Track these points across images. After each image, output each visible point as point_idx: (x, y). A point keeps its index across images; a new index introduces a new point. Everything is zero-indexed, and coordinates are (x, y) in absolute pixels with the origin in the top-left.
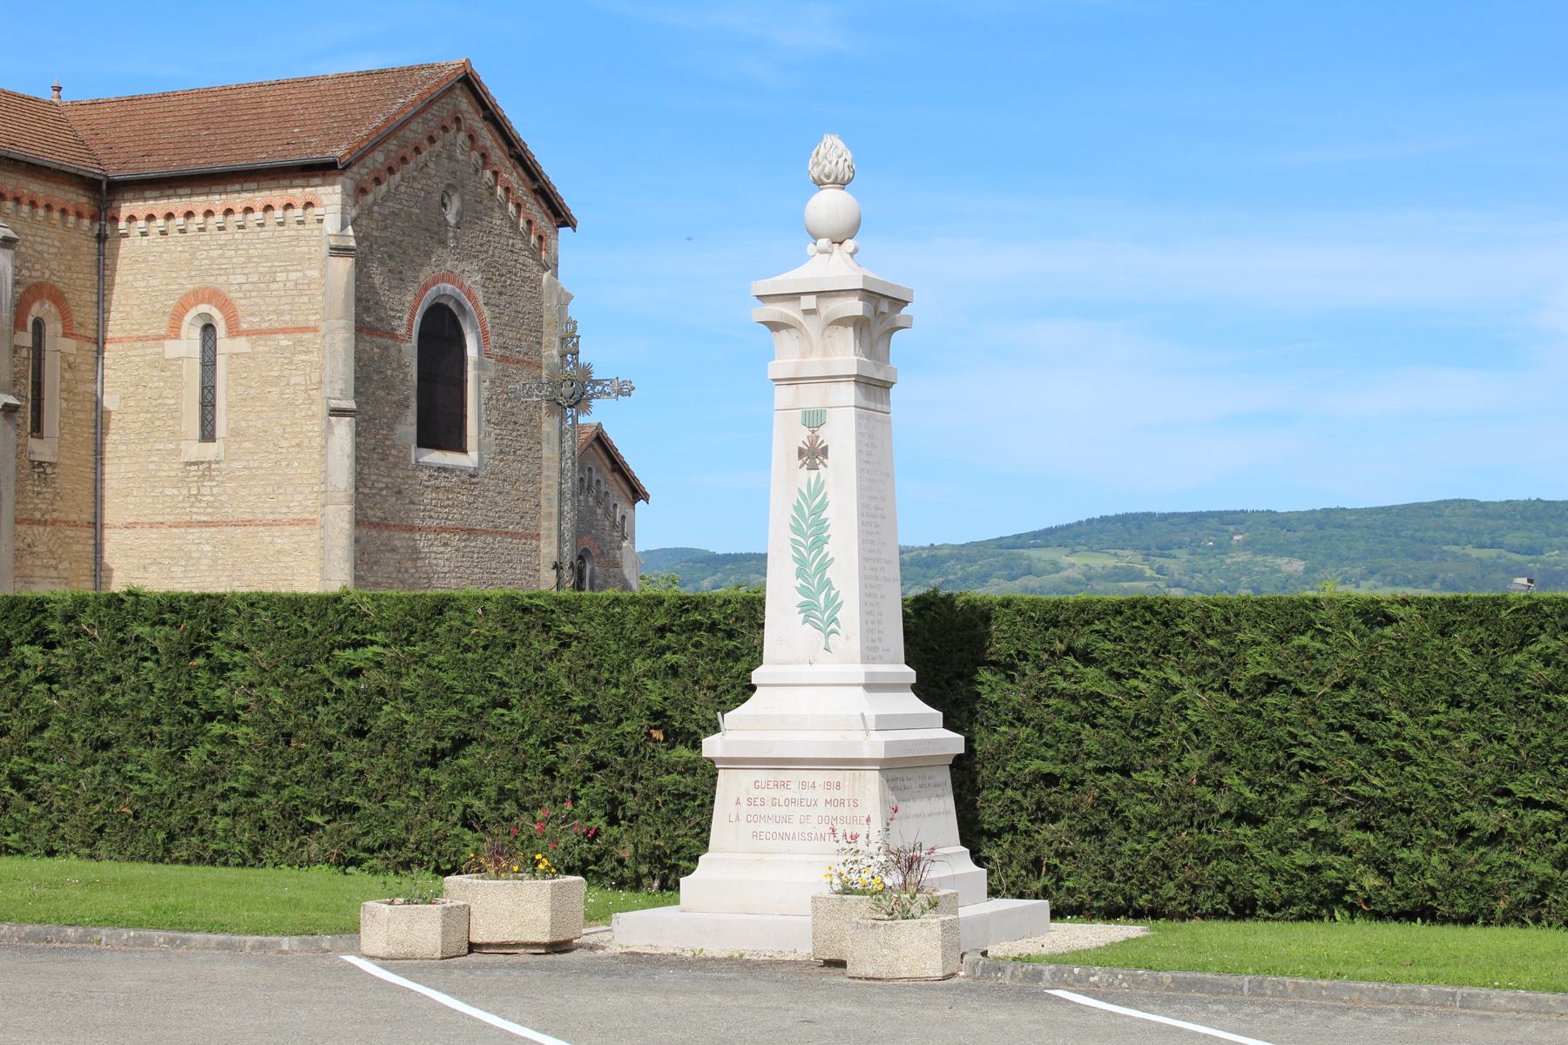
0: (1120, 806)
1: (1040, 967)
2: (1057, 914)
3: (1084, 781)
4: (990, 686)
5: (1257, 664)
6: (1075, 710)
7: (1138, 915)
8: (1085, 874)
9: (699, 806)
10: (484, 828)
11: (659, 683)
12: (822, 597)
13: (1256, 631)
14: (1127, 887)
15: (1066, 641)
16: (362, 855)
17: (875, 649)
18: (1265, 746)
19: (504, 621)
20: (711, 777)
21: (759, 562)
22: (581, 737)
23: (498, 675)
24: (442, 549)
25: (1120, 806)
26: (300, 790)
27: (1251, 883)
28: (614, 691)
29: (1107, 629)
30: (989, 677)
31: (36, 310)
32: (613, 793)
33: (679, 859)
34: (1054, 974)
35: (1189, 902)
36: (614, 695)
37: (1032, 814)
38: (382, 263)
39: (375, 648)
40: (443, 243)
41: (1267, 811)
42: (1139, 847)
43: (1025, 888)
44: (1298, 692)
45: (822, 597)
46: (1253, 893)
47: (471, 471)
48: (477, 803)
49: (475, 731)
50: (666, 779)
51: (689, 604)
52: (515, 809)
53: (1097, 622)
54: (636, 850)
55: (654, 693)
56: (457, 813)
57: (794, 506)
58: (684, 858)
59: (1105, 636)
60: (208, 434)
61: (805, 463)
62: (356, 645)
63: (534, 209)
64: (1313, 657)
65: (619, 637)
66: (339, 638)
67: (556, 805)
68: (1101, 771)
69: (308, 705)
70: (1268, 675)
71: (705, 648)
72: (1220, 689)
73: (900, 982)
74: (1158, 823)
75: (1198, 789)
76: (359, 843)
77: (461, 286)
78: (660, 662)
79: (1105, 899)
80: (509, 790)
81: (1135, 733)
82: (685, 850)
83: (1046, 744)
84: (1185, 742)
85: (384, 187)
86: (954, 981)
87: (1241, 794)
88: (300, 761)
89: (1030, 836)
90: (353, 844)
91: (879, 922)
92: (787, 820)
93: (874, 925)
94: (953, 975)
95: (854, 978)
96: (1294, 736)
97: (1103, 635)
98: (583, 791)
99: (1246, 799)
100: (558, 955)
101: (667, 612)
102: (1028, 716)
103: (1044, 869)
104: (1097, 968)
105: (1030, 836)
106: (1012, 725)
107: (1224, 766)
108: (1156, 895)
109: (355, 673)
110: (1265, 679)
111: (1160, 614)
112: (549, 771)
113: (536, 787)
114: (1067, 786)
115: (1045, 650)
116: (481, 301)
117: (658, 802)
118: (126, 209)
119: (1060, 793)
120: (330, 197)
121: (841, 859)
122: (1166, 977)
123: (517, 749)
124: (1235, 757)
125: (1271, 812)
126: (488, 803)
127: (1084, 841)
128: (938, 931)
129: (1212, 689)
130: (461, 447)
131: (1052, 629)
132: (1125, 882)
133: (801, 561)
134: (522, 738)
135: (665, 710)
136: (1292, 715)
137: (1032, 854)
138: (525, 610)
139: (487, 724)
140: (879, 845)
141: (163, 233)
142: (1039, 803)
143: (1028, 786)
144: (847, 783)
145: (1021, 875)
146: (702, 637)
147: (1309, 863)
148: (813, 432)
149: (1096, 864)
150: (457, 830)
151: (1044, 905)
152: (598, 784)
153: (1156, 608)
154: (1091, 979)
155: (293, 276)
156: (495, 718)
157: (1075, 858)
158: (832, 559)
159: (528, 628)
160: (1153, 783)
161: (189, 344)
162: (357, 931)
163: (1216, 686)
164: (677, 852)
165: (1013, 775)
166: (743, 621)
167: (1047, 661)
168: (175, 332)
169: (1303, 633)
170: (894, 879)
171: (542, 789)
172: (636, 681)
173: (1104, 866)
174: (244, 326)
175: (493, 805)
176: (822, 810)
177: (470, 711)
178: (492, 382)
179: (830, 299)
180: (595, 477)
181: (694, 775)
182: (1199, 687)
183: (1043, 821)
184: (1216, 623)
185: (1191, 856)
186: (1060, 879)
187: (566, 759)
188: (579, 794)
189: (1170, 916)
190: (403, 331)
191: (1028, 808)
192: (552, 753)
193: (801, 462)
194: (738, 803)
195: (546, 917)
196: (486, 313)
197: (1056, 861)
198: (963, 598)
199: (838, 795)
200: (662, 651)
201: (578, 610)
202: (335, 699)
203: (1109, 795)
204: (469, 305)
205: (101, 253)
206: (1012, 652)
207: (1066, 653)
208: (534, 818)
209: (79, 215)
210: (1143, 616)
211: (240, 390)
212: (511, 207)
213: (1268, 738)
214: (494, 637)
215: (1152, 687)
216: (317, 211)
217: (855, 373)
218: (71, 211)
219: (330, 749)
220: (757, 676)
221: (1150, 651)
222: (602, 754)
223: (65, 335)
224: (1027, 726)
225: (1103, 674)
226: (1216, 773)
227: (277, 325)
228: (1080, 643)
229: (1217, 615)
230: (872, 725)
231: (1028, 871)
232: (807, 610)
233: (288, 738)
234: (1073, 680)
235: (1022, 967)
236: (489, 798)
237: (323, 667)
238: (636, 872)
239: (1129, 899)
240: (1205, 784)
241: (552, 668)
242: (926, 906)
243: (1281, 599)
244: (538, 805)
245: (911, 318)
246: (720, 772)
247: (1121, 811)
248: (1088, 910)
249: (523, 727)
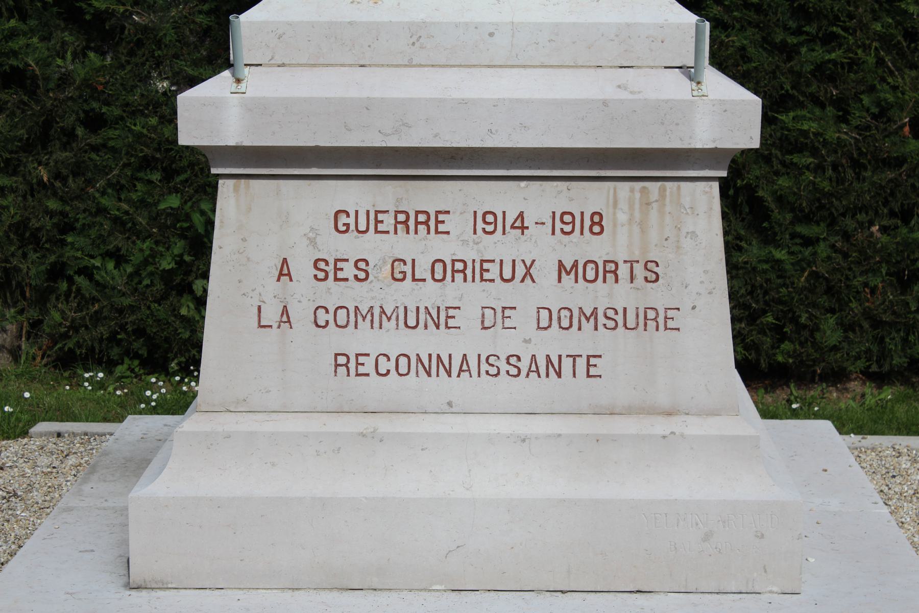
144: (622, 217)
194: (284, 272)
246: (225, 188)
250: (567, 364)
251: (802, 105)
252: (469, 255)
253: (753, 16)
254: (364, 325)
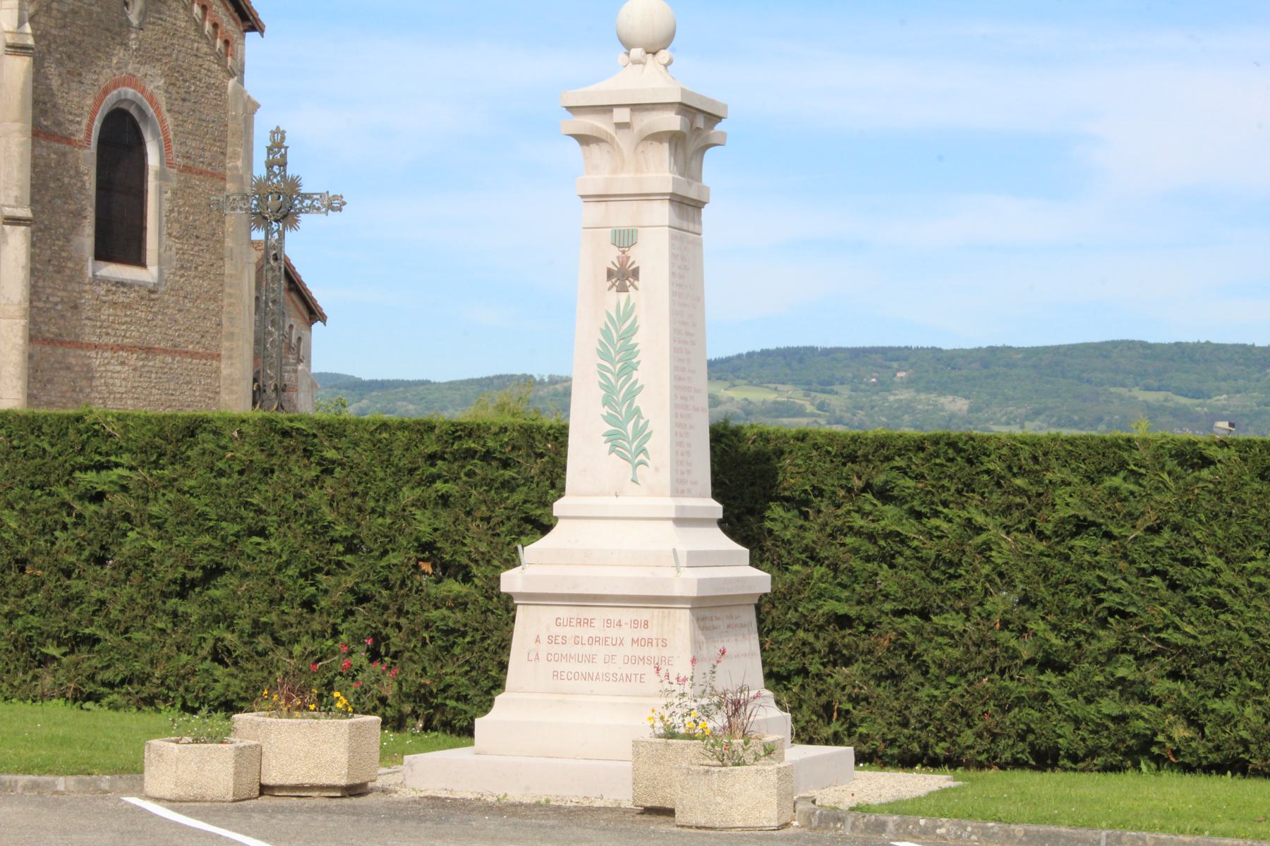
0: (919, 650)
1: (883, 818)
2: (862, 758)
3: (880, 623)
4: (782, 522)
5: (1067, 505)
6: (873, 550)
7: (934, 763)
8: (879, 720)
9: (468, 643)
10: (236, 663)
11: (428, 513)
12: (630, 426)
13: (1066, 471)
14: (923, 735)
15: (864, 478)
16: (102, 689)
17: (682, 482)
18: (1072, 591)
19: (262, 445)
20: (482, 613)
21: (561, 391)
22: (344, 568)
23: (255, 501)
24: (119, 368)
25: (919, 650)
26: (35, 620)
27: (1054, 732)
28: (380, 520)
29: (909, 466)
30: (782, 513)
32: (376, 628)
33: (446, 698)
34: (898, 826)
35: (987, 751)
36: (381, 525)
37: (825, 656)
38: (59, 63)
39: (120, 471)
41: (1073, 658)
42: (936, 693)
43: (815, 733)
44: (1109, 536)
45: (630, 426)
46: (1057, 743)
47: (151, 286)
48: (228, 636)
49: (227, 562)
50: (435, 614)
51: (461, 430)
52: (270, 643)
53: (897, 458)
54: (401, 689)
55: (423, 523)
56: (207, 647)
57: (601, 329)
58: (452, 698)
59: (906, 473)
61: (614, 285)
62: (99, 467)
64: (1125, 499)
65: (387, 463)
66: (80, 459)
67: (314, 640)
68: (899, 613)
69: (46, 530)
70: (1077, 517)
71: (478, 478)
72: (1027, 531)
73: (733, 832)
74: (958, 668)
75: (1001, 634)
76: (99, 678)
77: (143, 91)
78: (430, 490)
79: (900, 747)
80: (265, 624)
81: (935, 574)
82: (453, 688)
83: (840, 584)
84: (988, 585)
86: (790, 831)
87: (1047, 640)
88: (36, 590)
89: (821, 679)
90: (91, 678)
91: (713, 769)
92: (590, 659)
93: (707, 772)
94: (786, 825)
95: (683, 826)
96: (1104, 581)
97: (904, 471)
98: (345, 626)
99: (1051, 646)
100: (354, 799)
101: (439, 439)
102: (822, 555)
103: (835, 714)
104: (944, 820)
105: (821, 679)
106: (805, 564)
107: (1028, 610)
108: (954, 743)
109: (98, 497)
110: (1074, 521)
111: (964, 451)
112: (308, 605)
113: (292, 619)
114: (862, 628)
115: (842, 487)
116: (164, 108)
117: (425, 638)
119: (855, 636)
121: (664, 701)
122: (1019, 830)
123: (273, 581)
124: (1041, 601)
125: (1077, 660)
126: (241, 637)
127: (879, 685)
128: (774, 778)
129: (1018, 530)
130: (138, 259)
131: (849, 464)
132: (921, 729)
133: (609, 389)
134: (279, 569)
135: (435, 542)
136: (1102, 559)
137: (824, 699)
138: (285, 434)
139: (242, 553)
140: (703, 688)
142: (832, 646)
143: (821, 628)
145: (811, 720)
146: (475, 465)
147: (1116, 712)
148: (624, 252)
149: (891, 710)
150: (207, 664)
151: (846, 752)
152: (360, 619)
153: (960, 445)
154: (938, 831)
156: (250, 547)
157: (869, 703)
158: (642, 387)
159: (287, 453)
160: (953, 627)
162: (142, 772)
163: (1022, 527)
164: (444, 691)
165: (805, 616)
166: (520, 449)
167: (844, 497)
169: (1115, 474)
170: (720, 720)
171: (299, 623)
172: (404, 510)
173: (900, 712)
175: (246, 639)
176: (628, 650)
177: (223, 539)
178: (174, 193)
179: (645, 113)
181: (465, 610)
182: (1004, 528)
183: (835, 664)
184: (1024, 462)
185: (992, 703)
186: (853, 725)
187: (326, 592)
188: (340, 629)
189: (967, 766)
190: (81, 136)
191: (820, 652)
192: (312, 585)
193: (609, 283)
194: (538, 640)
195: (343, 758)
196: (169, 120)
197: (849, 706)
198: (755, 430)
199: (645, 634)
200: (432, 479)
201: (341, 435)
202: (75, 525)
203: (907, 638)
204: (151, 111)
206: (807, 487)
207: (864, 490)
208: (291, 653)
210: (946, 453)
213: (1075, 582)
214: (251, 461)
215: (955, 527)
217: (670, 191)
219: (69, 577)
220: (559, 507)
221: (953, 489)
222: (365, 587)
224: (821, 565)
225: (903, 513)
226: (1019, 618)
228: (879, 480)
229: (1025, 453)
230: (683, 561)
231: (820, 716)
232: (614, 439)
233: (21, 564)
234: (870, 518)
235: (864, 817)
236: (242, 631)
237: (62, 490)
238: (400, 711)
239: (925, 747)
240: (1008, 628)
241: (314, 495)
242: (762, 753)
243: (1093, 438)
244: (295, 640)
245: (724, 135)
246: (519, 608)
247: (919, 655)
248: (880, 758)
249: (280, 557)
250: (633, 677)
251: (948, 611)
252: (602, 635)
253: (920, 564)
254: (564, 661)
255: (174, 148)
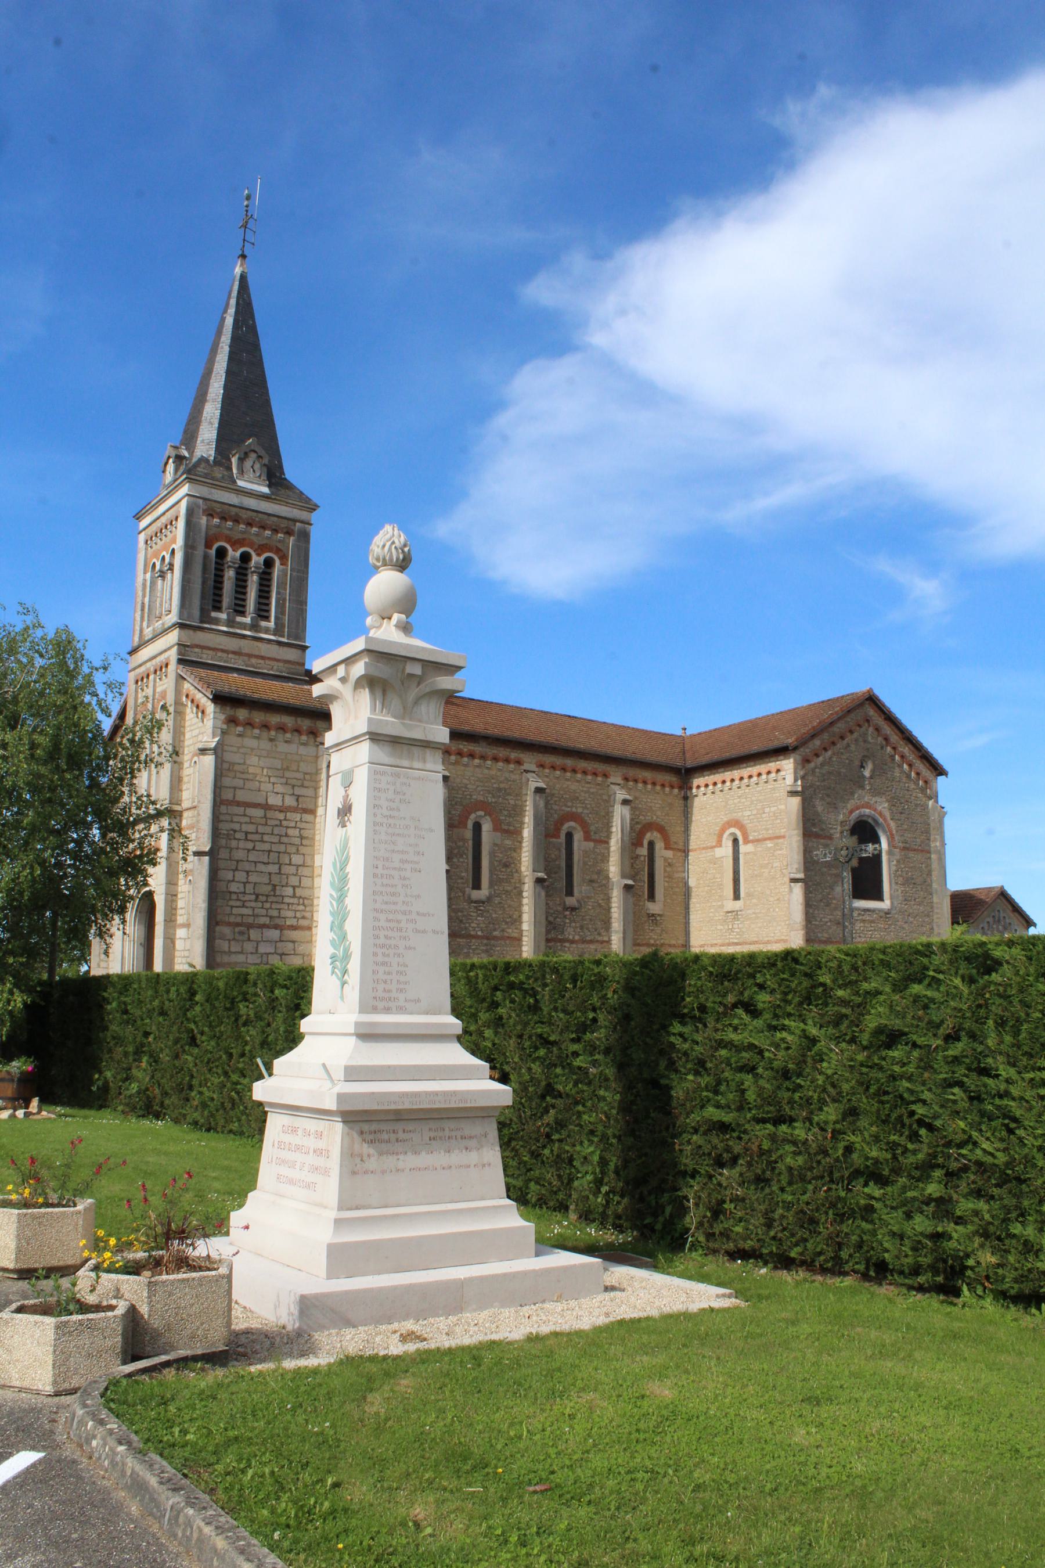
18: (888, 1102)
31: (648, 836)
38: (822, 799)
40: (862, 787)
60: (737, 896)
63: (920, 766)
77: (875, 810)
85: (821, 759)
116: (888, 818)
118: (696, 782)
120: (788, 765)
130: (879, 897)
141: (713, 793)
147: (930, 1230)
155: (773, 809)
161: (727, 849)
168: (719, 844)
174: (751, 838)
178: (898, 861)
180: (1002, 915)
196: (892, 824)
204: (881, 820)
205: (686, 806)
209: (672, 787)
211: (750, 872)
212: (905, 766)
216: (782, 773)
218: (667, 785)
223: (666, 849)
227: (766, 836)
255: (896, 838)
